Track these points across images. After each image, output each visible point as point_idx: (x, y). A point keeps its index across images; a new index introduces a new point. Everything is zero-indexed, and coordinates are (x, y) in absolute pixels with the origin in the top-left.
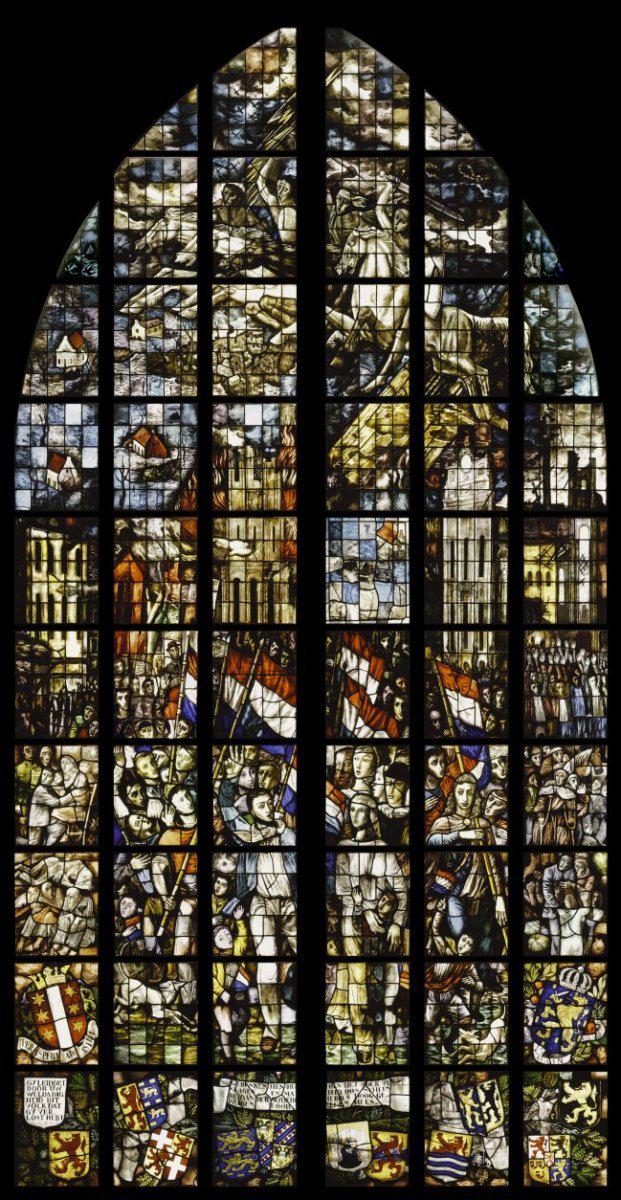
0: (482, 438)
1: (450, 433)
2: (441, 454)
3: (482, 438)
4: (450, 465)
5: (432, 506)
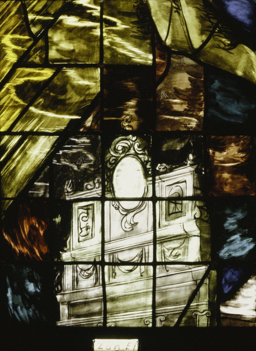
0: (178, 104)
1: (80, 90)
2: (52, 155)
3: (178, 104)
4: (78, 187)
5: (23, 313)
